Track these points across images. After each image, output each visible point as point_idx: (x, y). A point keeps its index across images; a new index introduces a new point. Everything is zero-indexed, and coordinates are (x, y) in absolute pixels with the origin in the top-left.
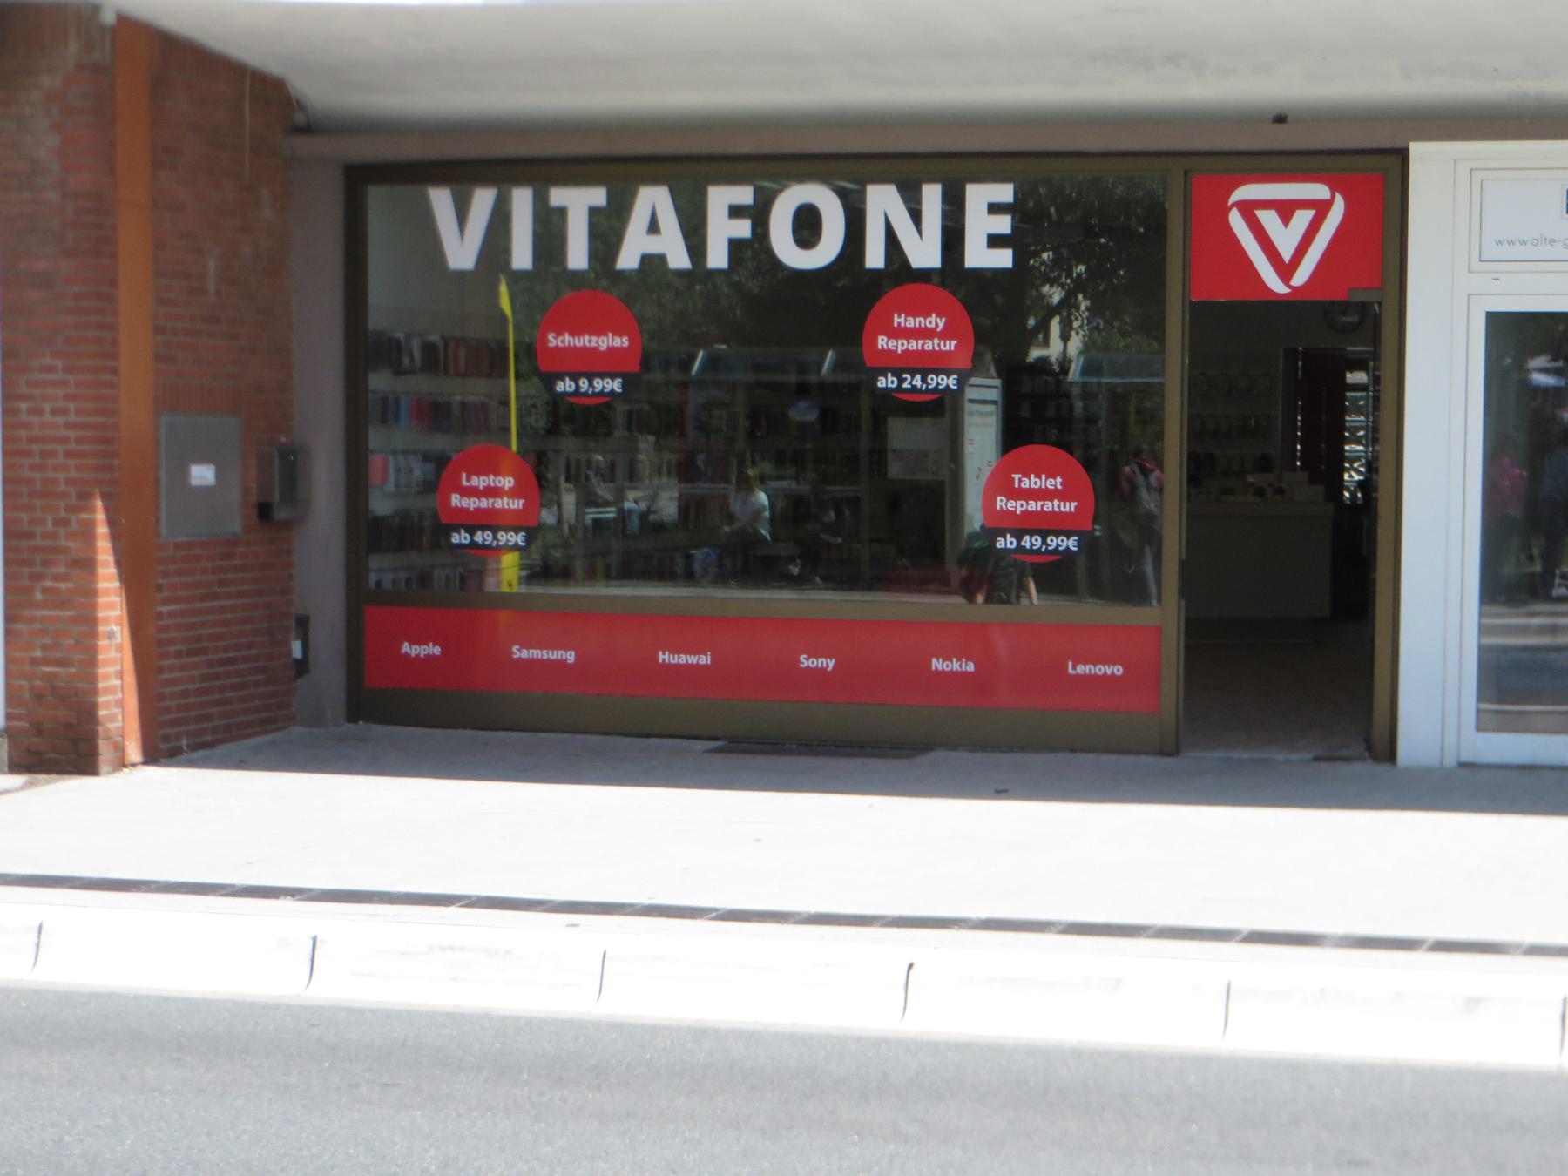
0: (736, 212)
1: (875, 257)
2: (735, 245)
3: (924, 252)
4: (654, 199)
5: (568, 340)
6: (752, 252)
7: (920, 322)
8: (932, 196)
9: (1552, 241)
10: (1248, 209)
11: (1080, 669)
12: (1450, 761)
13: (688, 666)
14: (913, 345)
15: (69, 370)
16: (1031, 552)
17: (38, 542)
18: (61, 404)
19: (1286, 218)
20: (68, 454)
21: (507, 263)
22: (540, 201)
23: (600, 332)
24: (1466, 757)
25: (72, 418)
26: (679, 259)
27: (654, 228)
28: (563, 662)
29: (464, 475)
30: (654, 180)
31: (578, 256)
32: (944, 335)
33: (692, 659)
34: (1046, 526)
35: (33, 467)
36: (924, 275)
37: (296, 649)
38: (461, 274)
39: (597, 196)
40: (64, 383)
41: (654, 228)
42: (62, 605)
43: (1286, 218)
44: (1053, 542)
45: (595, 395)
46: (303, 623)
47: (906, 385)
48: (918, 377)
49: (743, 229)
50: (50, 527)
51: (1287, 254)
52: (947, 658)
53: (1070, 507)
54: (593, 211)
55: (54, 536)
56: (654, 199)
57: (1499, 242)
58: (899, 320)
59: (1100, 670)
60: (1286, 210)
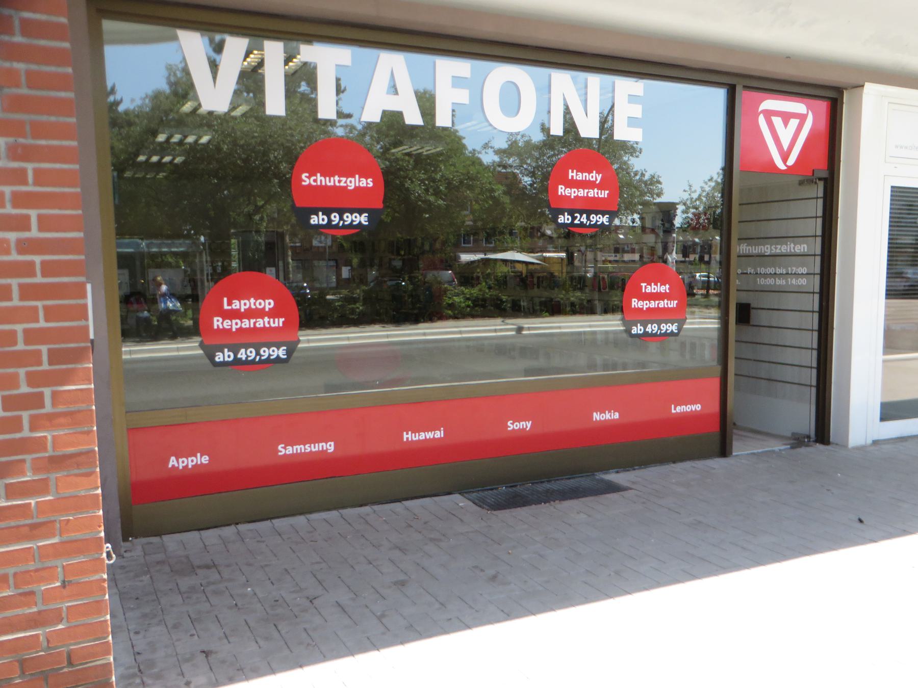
5: (320, 180)
10: (769, 114)
11: (679, 409)
12: (869, 441)
19: (786, 124)
20: (27, 292)
25: (34, 233)
29: (225, 300)
33: (430, 435)
41: (394, 90)
42: (36, 530)
43: (786, 124)
45: (344, 227)
47: (576, 222)
48: (585, 216)
49: (463, 96)
51: (785, 147)
57: (897, 147)
58: (572, 174)
60: (786, 117)
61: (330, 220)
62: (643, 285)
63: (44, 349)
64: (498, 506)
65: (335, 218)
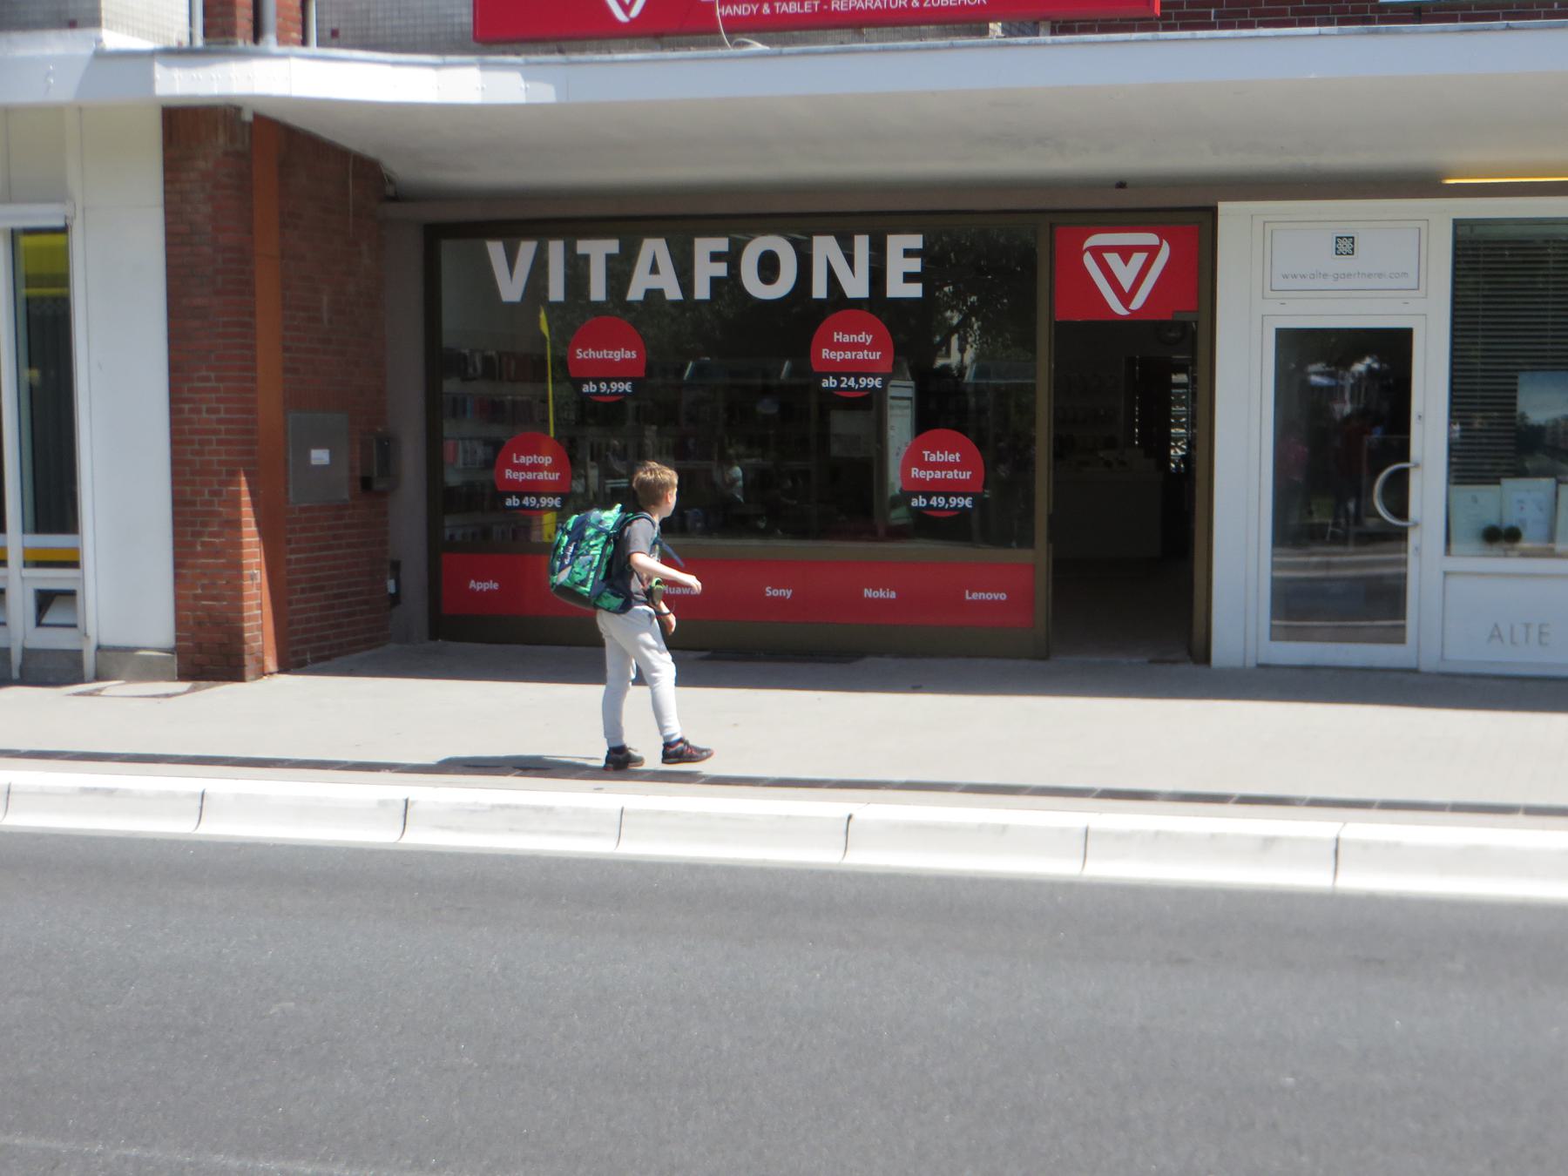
0: (715, 257)
1: (819, 290)
2: (715, 282)
3: (856, 286)
4: (654, 248)
5: (592, 354)
6: (728, 286)
7: (853, 338)
8: (862, 244)
9: (1325, 275)
10: (1097, 252)
11: (975, 596)
12: (1251, 663)
14: (849, 355)
15: (219, 379)
18: (214, 405)
20: (220, 442)
21: (546, 297)
22: (570, 251)
24: (1262, 660)
25: (222, 415)
26: (673, 293)
27: (654, 269)
30: (655, 234)
31: (598, 292)
32: (871, 348)
34: (948, 489)
36: (857, 303)
37: (391, 586)
38: (512, 305)
39: (613, 246)
41: (654, 269)
42: (217, 554)
44: (953, 501)
45: (612, 394)
46: (396, 567)
49: (721, 269)
50: (207, 497)
51: (1127, 285)
52: (875, 588)
53: (966, 475)
54: (610, 258)
55: (210, 503)
57: (1285, 277)
59: (989, 596)
65: (603, 386)
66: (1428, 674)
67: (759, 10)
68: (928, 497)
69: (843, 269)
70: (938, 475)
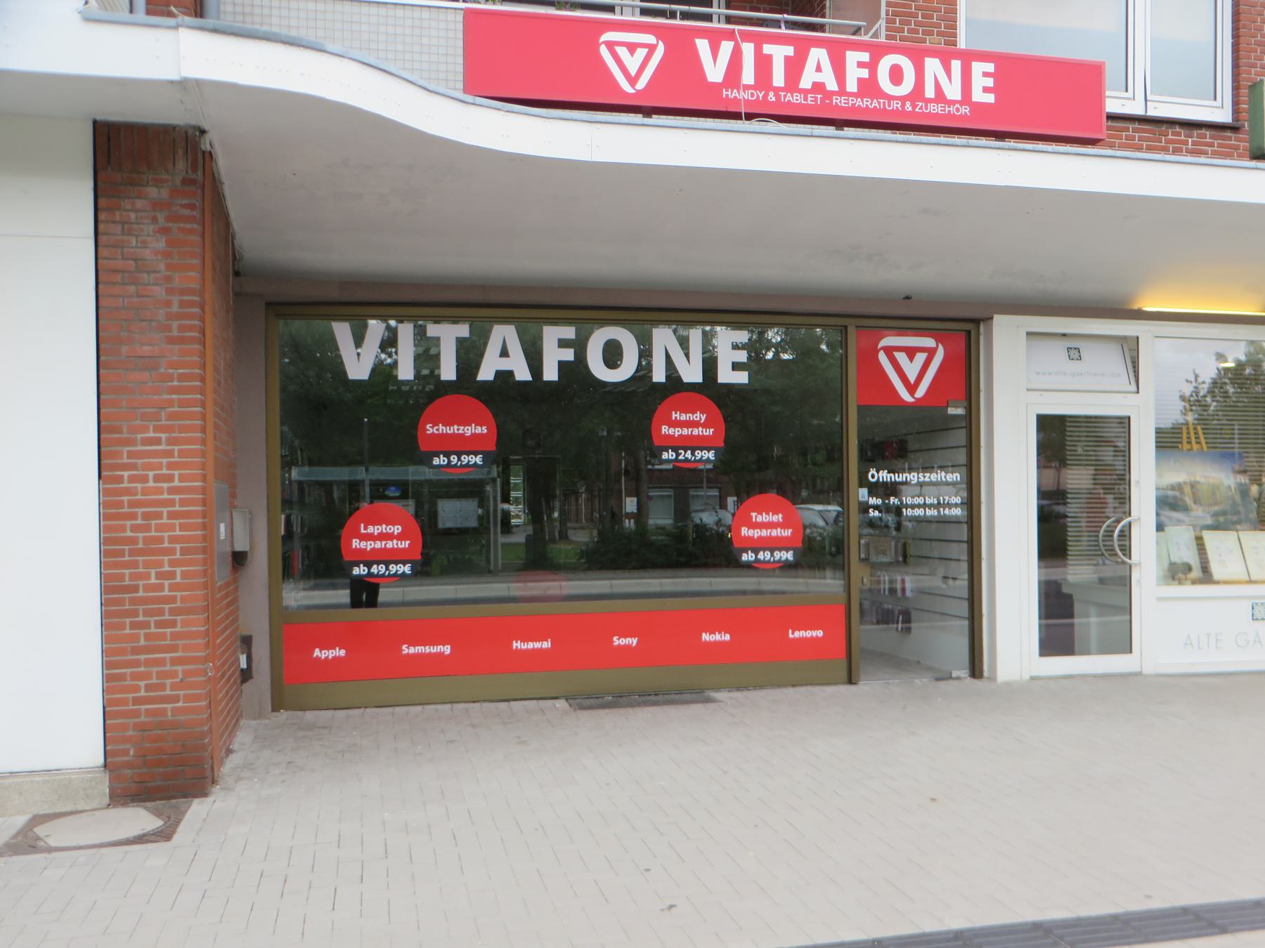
0: (563, 344)
1: (659, 376)
3: (692, 373)
5: (442, 429)
6: (575, 371)
10: (889, 351)
11: (797, 634)
12: (1026, 677)
13: (534, 650)
14: (685, 432)
15: (171, 442)
16: (764, 562)
17: (141, 594)
19: (911, 358)
20: (172, 515)
22: (420, 334)
23: (466, 423)
24: (1035, 674)
25: (176, 483)
26: (523, 374)
27: (504, 353)
28: (441, 654)
31: (448, 371)
32: (705, 425)
33: (537, 645)
34: (773, 545)
35: (135, 528)
36: (693, 387)
39: (463, 330)
40: (169, 454)
41: (504, 353)
43: (911, 358)
50: (153, 580)
53: (787, 533)
54: (460, 342)
55: (160, 587)
56: (504, 334)
58: (675, 415)
59: (809, 634)
60: (911, 352)
61: (449, 461)
62: (754, 514)
63: (178, 546)
64: (582, 708)
65: (454, 459)
66: (1150, 676)
67: (765, 96)
68: (756, 552)
69: (677, 354)
70: (764, 533)
